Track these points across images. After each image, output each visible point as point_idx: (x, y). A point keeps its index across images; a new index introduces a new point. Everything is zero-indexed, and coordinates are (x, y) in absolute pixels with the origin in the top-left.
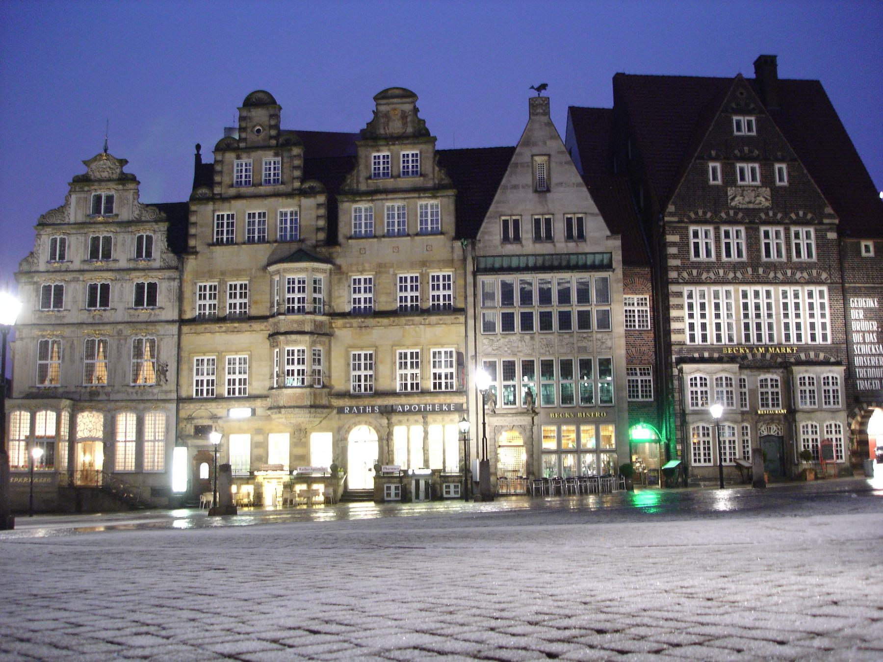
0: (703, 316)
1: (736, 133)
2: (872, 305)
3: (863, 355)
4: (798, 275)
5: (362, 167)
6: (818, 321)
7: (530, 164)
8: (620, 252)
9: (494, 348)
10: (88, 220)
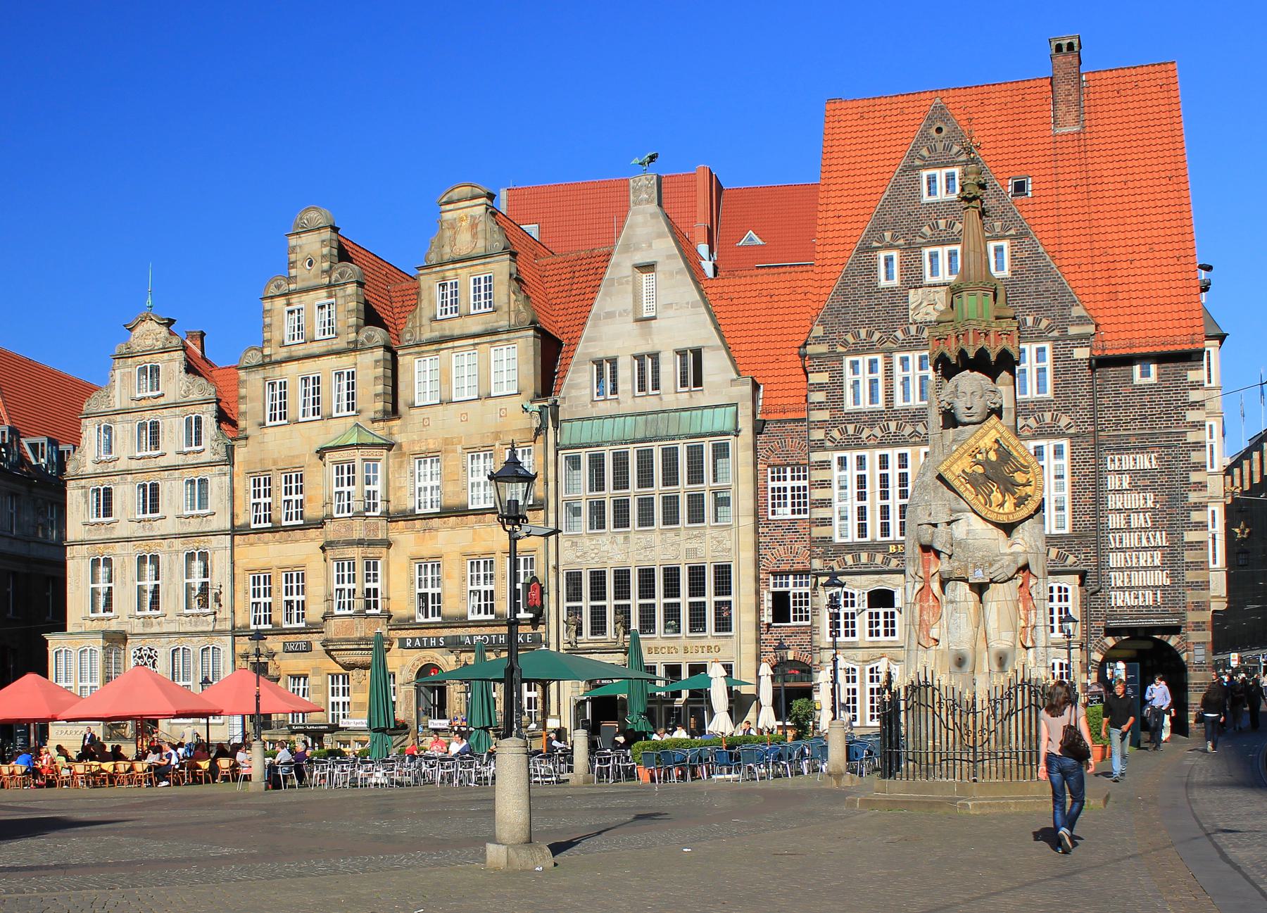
2: (1147, 465)
5: (425, 304)
7: (630, 279)
9: (578, 554)
10: (133, 405)
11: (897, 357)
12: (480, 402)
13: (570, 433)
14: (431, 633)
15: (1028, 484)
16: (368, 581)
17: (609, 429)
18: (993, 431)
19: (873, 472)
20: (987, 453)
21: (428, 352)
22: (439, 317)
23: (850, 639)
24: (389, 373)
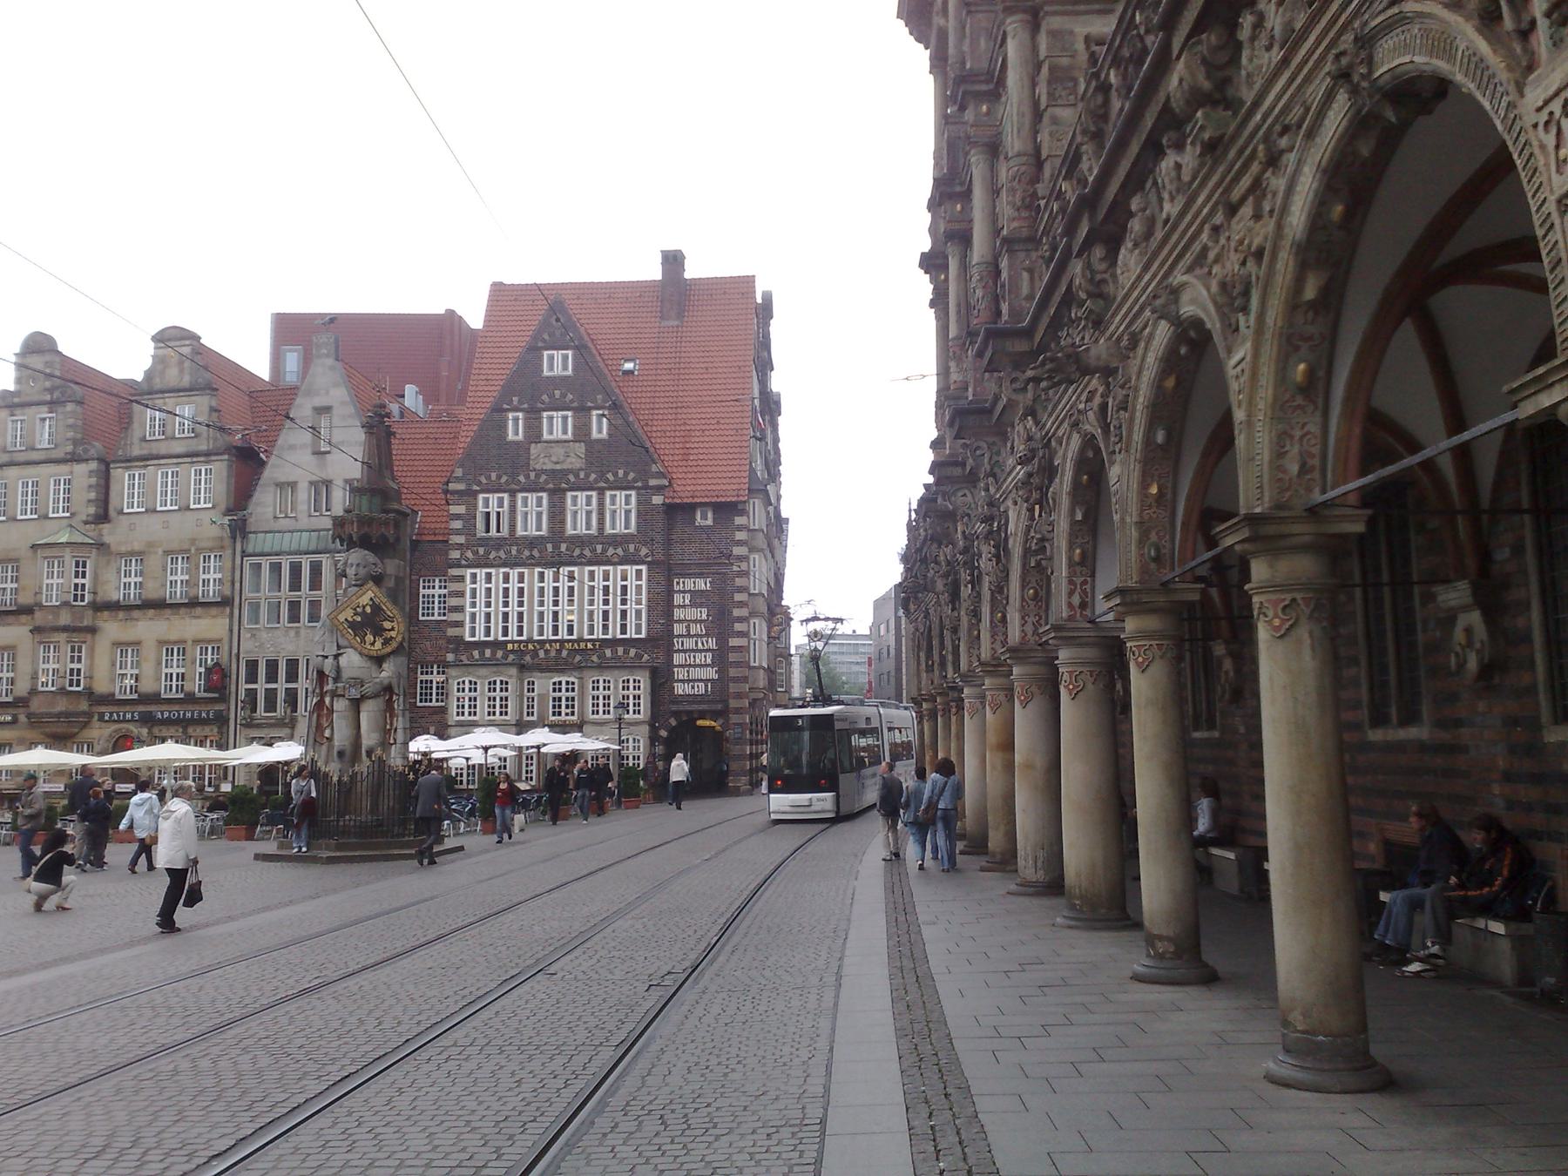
0: (488, 605)
1: (546, 373)
3: (685, 651)
4: (611, 551)
5: (136, 425)
6: (631, 607)
12: (180, 513)
13: (256, 542)
14: (128, 708)
15: (393, 629)
16: (72, 662)
17: (287, 542)
18: (370, 592)
19: (497, 584)
20: (364, 607)
21: (136, 466)
22: (148, 438)
23: (472, 718)
24: (102, 482)
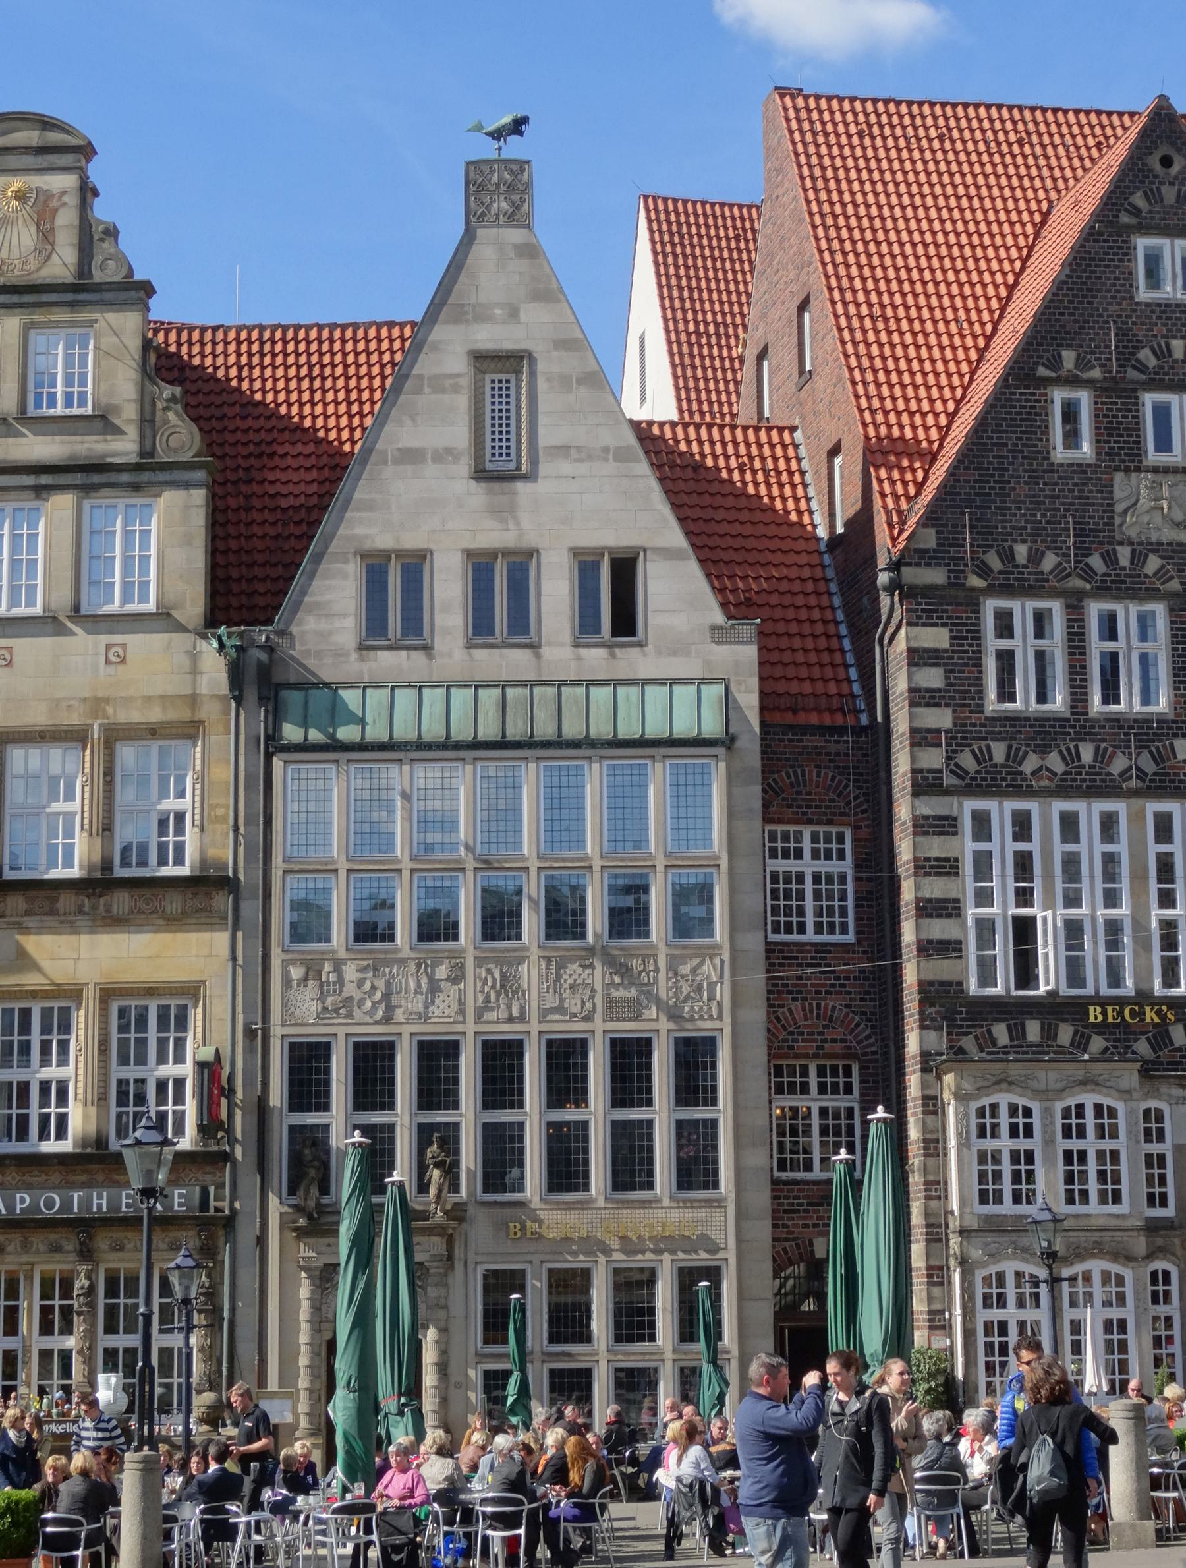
1: (1144, 294)
7: (465, 382)
8: (754, 682)
11: (1094, 609)
23: (1023, 1209)
